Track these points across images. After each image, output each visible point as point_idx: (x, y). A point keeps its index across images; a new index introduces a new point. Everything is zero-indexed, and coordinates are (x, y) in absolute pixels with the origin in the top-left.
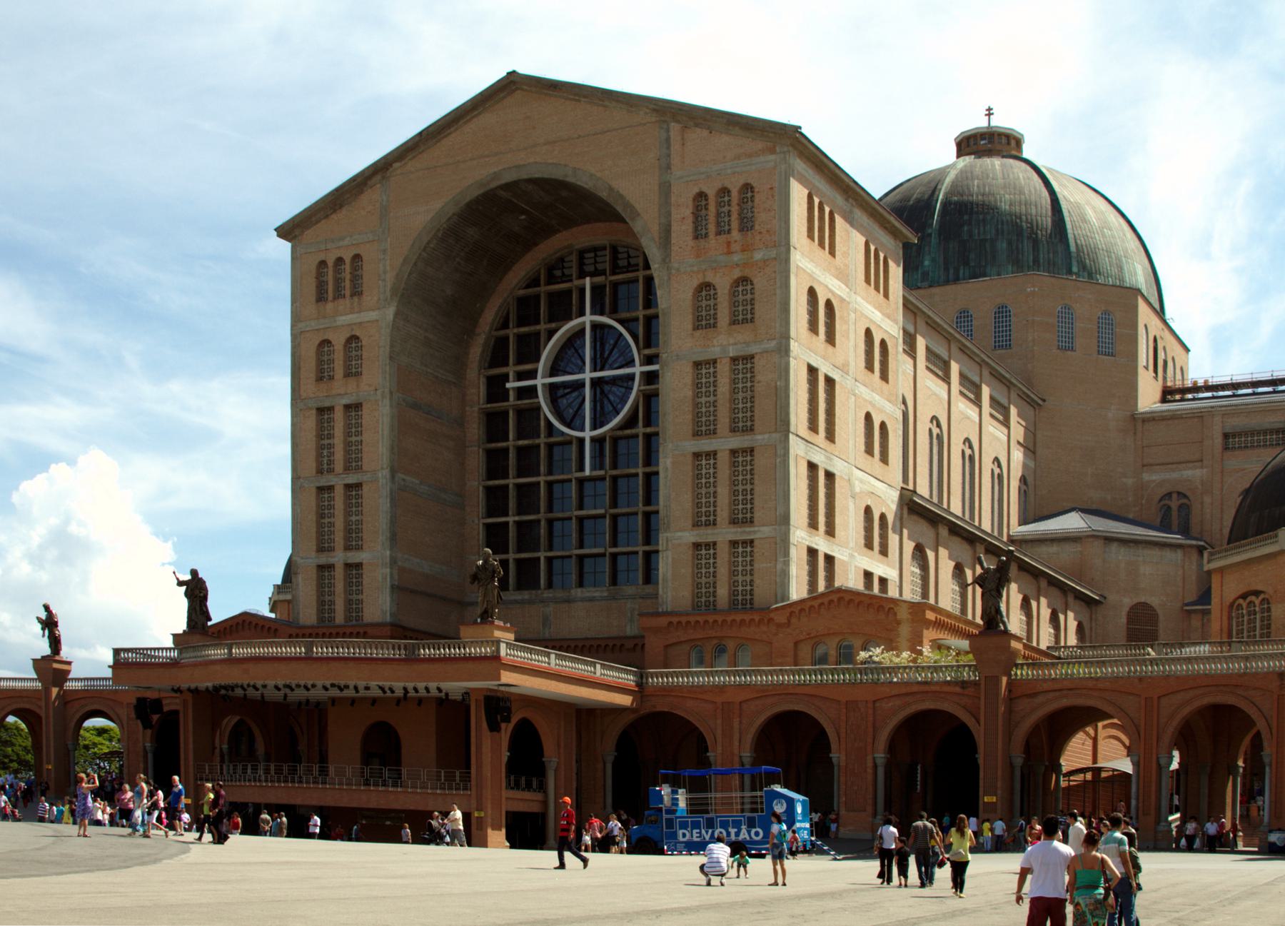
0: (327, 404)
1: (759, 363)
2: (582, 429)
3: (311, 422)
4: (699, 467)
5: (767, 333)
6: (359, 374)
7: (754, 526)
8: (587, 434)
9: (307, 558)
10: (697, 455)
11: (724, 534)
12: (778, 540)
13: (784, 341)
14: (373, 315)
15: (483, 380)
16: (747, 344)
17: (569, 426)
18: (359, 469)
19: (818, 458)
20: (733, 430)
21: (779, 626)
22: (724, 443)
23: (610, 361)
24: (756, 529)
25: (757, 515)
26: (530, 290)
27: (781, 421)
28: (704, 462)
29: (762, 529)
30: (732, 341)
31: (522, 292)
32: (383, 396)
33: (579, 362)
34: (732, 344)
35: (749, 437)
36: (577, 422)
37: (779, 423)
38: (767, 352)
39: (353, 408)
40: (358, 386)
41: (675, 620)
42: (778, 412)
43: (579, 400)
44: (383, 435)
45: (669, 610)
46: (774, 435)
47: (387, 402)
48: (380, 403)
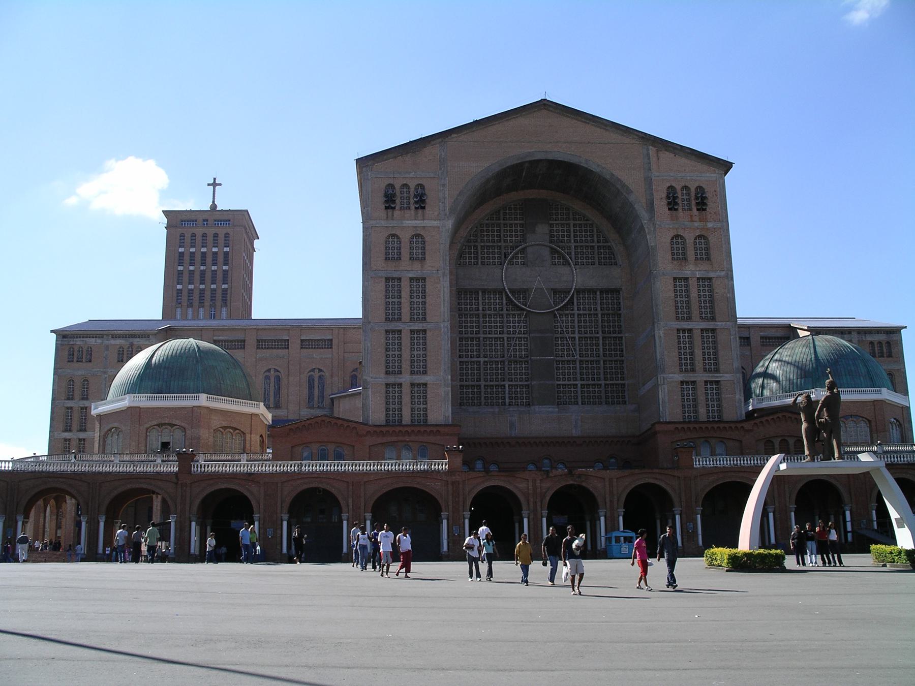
0: (395, 275)
1: (716, 283)
3: (381, 286)
5: (719, 267)
6: (424, 259)
7: (720, 373)
10: (678, 330)
11: (701, 377)
13: (729, 273)
22: (697, 325)
24: (721, 375)
25: (722, 367)
27: (732, 316)
28: (681, 335)
29: (725, 375)
30: (698, 269)
32: (444, 274)
34: (698, 271)
35: (713, 323)
37: (730, 316)
38: (720, 277)
40: (422, 267)
41: (680, 426)
42: (730, 311)
44: (444, 300)
45: (667, 421)
46: (728, 323)
47: (447, 279)
48: (441, 279)
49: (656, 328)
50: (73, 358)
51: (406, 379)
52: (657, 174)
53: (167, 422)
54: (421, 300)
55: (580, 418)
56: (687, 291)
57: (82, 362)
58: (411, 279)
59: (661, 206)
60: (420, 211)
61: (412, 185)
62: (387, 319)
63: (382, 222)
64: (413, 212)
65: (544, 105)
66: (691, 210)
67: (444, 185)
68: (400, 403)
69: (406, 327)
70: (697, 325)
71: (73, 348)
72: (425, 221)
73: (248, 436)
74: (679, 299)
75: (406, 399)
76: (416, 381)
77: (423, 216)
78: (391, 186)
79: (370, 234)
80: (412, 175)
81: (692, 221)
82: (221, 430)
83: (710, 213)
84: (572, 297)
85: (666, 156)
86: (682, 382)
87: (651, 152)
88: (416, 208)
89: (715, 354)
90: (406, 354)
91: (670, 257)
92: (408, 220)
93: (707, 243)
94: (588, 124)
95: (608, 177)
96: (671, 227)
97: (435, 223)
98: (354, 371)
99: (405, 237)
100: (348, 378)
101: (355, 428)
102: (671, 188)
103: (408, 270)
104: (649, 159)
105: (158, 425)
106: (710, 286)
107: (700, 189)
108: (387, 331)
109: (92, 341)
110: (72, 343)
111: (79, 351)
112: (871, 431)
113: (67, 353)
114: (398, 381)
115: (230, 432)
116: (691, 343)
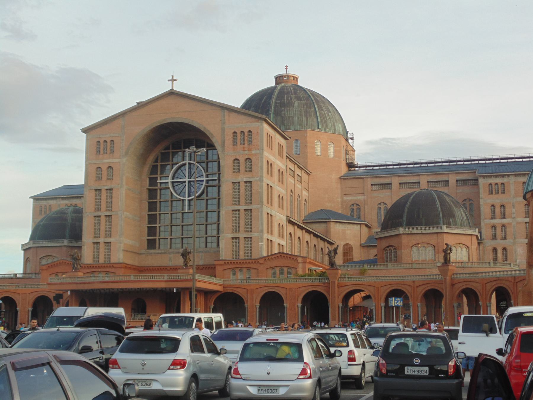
4: (233, 214)
10: (233, 210)
11: (242, 235)
12: (260, 237)
14: (117, 160)
15: (148, 179)
17: (179, 195)
19: (269, 212)
20: (245, 204)
21: (261, 264)
22: (242, 208)
23: (194, 175)
25: (253, 229)
26: (166, 151)
30: (245, 177)
31: (163, 151)
33: (183, 175)
36: (182, 194)
41: (226, 262)
43: (183, 186)
45: (223, 259)
46: (258, 206)
51: (101, 240)
55: (203, 255)
56: (239, 189)
58: (107, 189)
59: (229, 142)
61: (108, 141)
62: (95, 211)
65: (172, 93)
66: (244, 144)
69: (102, 214)
70: (242, 208)
74: (235, 194)
80: (108, 136)
81: (244, 151)
83: (254, 145)
87: (226, 114)
89: (251, 222)
90: (103, 227)
91: (231, 170)
92: (106, 159)
93: (251, 162)
96: (233, 154)
97: (117, 160)
99: (104, 168)
104: (224, 117)
105: (45, 256)
106: (251, 186)
112: (435, 252)
114: (98, 241)
116: (239, 217)
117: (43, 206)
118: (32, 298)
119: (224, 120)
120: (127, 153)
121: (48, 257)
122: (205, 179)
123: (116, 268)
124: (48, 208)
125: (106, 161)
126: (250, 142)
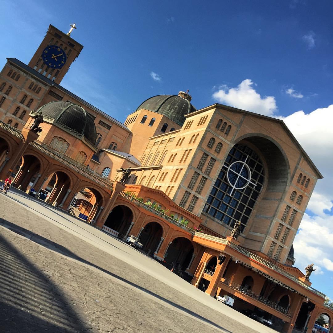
0: (207, 153)
1: (298, 214)
2: (233, 185)
3: (201, 155)
6: (219, 153)
8: (234, 187)
9: (184, 187)
11: (279, 243)
16: (297, 209)
18: (208, 175)
22: (286, 225)
39: (214, 160)
44: (218, 172)
46: (295, 230)
49: (274, 219)
50: (10, 75)
52: (300, 167)
53: (64, 138)
54: (210, 167)
57: (13, 78)
58: (212, 158)
59: (296, 178)
60: (226, 135)
61: (228, 124)
63: (213, 132)
64: (224, 134)
67: (237, 131)
68: (187, 200)
69: (202, 174)
70: (286, 225)
71: (12, 71)
72: (226, 140)
73: (87, 158)
75: (190, 200)
76: (196, 196)
77: (226, 137)
78: (221, 120)
79: (207, 133)
81: (301, 189)
82: (81, 152)
84: (245, 188)
85: (305, 163)
86: (273, 242)
88: (225, 134)
94: (289, 137)
95: (286, 159)
98: (112, 143)
99: (217, 141)
100: (109, 144)
101: (170, 202)
102: (301, 174)
103: (212, 153)
104: (300, 160)
105: (59, 137)
107: (309, 179)
108: (195, 172)
109: (22, 73)
110: (13, 68)
111: (14, 74)
113: (9, 71)
115: (83, 154)
117: (13, 72)
118: (148, 220)
119: (299, 162)
120: (236, 141)
121: (61, 140)
122: (249, 181)
123: (197, 220)
124: (17, 75)
125: (220, 137)
126: (307, 186)
